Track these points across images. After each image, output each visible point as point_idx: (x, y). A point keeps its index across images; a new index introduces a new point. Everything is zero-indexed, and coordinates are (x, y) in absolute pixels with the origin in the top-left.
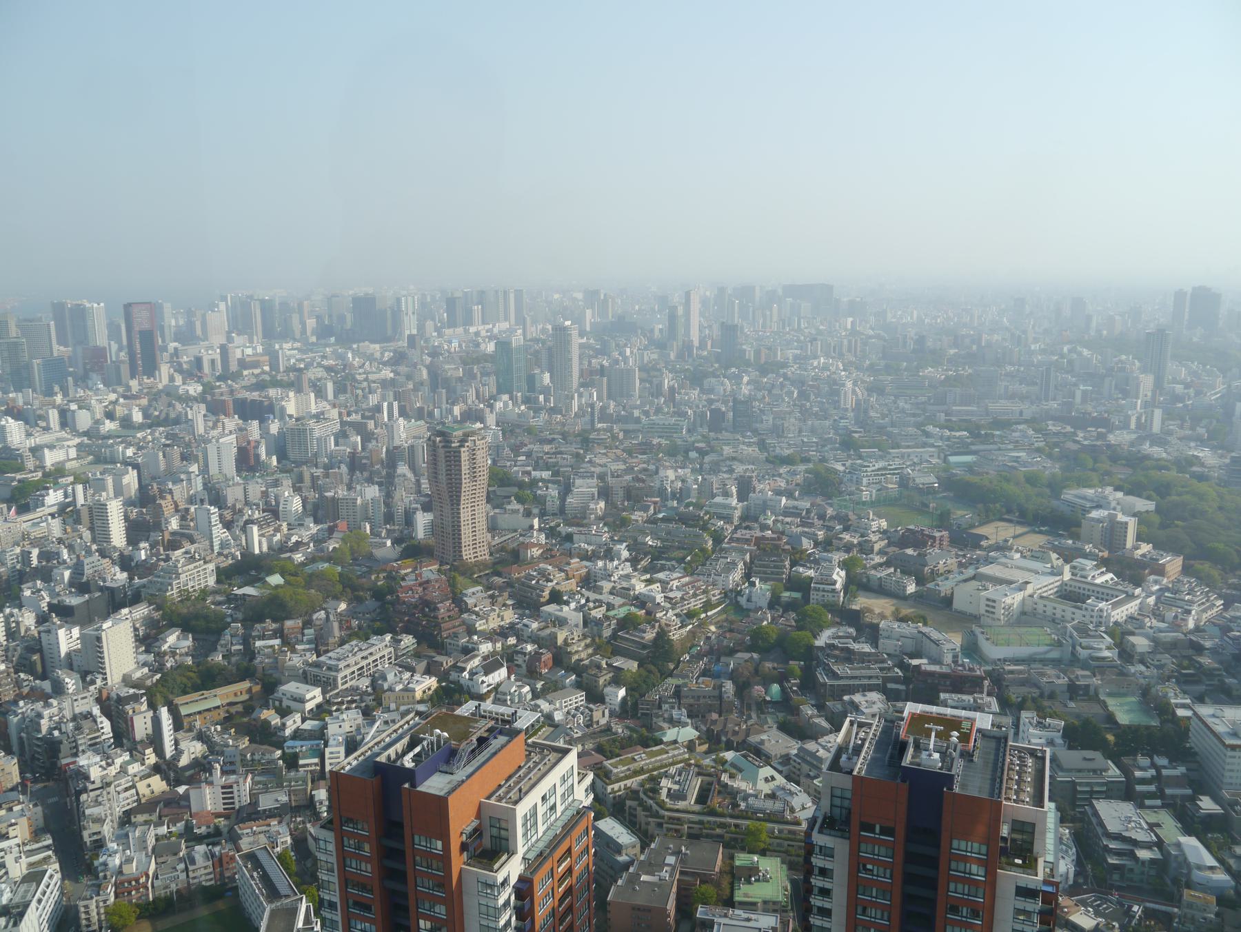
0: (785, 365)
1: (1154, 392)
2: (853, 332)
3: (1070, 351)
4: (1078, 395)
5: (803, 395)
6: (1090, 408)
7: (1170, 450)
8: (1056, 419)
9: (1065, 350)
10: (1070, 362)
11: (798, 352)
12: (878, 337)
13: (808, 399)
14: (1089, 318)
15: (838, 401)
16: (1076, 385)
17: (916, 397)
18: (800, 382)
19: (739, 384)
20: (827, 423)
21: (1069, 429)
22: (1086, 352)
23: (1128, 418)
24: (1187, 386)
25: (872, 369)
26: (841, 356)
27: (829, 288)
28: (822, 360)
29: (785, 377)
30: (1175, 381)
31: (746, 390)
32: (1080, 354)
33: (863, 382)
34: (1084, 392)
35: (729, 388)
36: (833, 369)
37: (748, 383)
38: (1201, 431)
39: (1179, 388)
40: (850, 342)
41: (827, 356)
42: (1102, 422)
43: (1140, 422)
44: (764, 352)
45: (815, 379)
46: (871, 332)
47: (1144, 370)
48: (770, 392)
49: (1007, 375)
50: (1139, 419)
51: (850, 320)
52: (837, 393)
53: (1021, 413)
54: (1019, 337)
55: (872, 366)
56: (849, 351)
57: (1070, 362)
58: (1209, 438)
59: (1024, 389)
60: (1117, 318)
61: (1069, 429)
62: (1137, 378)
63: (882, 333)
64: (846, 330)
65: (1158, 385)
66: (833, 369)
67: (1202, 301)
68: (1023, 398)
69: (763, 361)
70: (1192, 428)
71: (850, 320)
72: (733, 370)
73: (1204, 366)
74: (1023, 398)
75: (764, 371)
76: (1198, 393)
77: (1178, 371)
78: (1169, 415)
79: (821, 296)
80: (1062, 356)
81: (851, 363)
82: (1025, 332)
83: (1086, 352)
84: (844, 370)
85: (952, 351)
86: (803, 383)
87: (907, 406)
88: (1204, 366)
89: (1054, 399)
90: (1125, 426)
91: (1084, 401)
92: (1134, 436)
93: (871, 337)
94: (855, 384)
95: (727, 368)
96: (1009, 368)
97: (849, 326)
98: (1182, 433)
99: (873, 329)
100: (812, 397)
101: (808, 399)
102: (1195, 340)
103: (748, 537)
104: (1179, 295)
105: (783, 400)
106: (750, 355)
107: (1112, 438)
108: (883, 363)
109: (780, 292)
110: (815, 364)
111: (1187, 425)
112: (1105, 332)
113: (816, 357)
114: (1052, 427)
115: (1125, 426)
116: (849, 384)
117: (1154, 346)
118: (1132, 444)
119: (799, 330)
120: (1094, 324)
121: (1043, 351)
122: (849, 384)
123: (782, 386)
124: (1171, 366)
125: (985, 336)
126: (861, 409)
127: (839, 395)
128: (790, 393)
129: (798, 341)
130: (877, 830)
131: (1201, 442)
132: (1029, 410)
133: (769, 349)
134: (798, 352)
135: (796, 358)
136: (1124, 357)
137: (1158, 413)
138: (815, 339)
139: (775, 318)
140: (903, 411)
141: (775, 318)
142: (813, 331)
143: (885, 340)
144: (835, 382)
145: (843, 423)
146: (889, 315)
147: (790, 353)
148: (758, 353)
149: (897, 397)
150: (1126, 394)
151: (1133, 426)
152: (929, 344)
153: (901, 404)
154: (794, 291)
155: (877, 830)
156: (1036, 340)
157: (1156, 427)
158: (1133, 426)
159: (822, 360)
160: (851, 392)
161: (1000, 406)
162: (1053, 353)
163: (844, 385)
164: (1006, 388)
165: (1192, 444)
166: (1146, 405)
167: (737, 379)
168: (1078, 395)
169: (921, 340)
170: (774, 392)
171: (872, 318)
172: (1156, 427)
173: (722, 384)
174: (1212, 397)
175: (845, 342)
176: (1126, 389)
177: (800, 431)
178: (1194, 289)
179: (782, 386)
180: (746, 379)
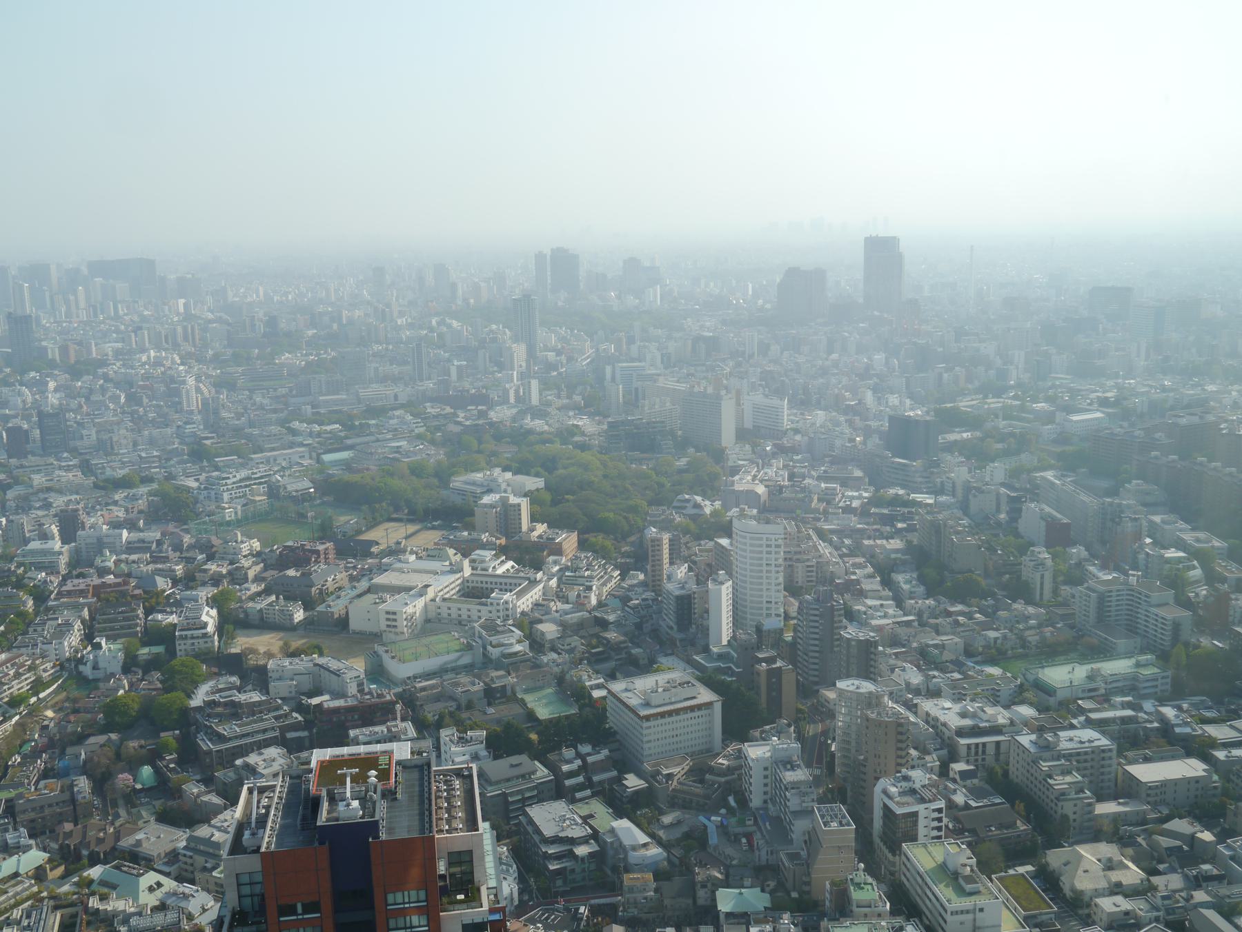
0: (103, 363)
1: (528, 361)
2: (188, 316)
3: (439, 324)
5: (133, 399)
6: (467, 385)
8: (432, 400)
9: (434, 322)
10: (440, 336)
11: (120, 345)
12: (219, 320)
13: (140, 404)
14: (454, 286)
15: (180, 403)
16: (449, 360)
17: (275, 390)
18: (127, 384)
19: (43, 392)
20: (169, 431)
21: (448, 410)
22: (455, 324)
23: (506, 392)
24: (559, 353)
25: (217, 360)
26: (176, 346)
27: (149, 264)
28: (152, 353)
29: (106, 378)
30: (546, 349)
31: (53, 399)
32: (449, 326)
33: (208, 376)
35: (30, 399)
36: (168, 363)
37: (56, 390)
39: (551, 356)
40: (185, 328)
41: (158, 348)
42: (481, 399)
43: (518, 394)
44: (73, 349)
45: (146, 377)
46: (210, 316)
47: (516, 339)
48: (87, 399)
49: (374, 355)
50: (517, 392)
51: (182, 301)
52: (177, 392)
53: (396, 397)
54: (383, 311)
55: (216, 356)
56: (186, 339)
57: (440, 336)
58: (586, 406)
59: (395, 369)
60: (483, 284)
61: (448, 410)
62: (510, 348)
63: (225, 317)
64: (178, 314)
66: (168, 363)
67: (561, 264)
68: (396, 380)
69: (72, 360)
70: (569, 397)
71: (182, 301)
72: (32, 374)
73: (572, 330)
74: (396, 380)
75: (75, 373)
76: (570, 359)
77: (547, 337)
78: (545, 385)
79: (141, 274)
80: (431, 330)
81: (190, 355)
82: (388, 305)
83: (455, 324)
84: (182, 364)
85: (310, 333)
86: (131, 385)
87: (266, 401)
88: (572, 330)
89: (429, 379)
90: (505, 401)
91: (460, 378)
92: (514, 411)
93: (210, 321)
94: (198, 379)
95: (24, 372)
96: (376, 347)
97: (181, 309)
98: (560, 403)
99: (212, 312)
100: (145, 400)
101: (140, 404)
102: (560, 304)
103: (82, 587)
104: (540, 257)
105: (107, 408)
106: (54, 353)
108: (229, 351)
109: (85, 270)
110: (144, 358)
111: (564, 394)
112: (472, 301)
113: (143, 350)
114: (431, 410)
115: (505, 401)
116: (191, 381)
117: (522, 313)
118: (514, 419)
119: (117, 317)
120: (460, 292)
121: (410, 326)
122: (191, 381)
123: (103, 390)
124: (541, 333)
125: (345, 313)
126: (210, 410)
127: (180, 396)
128: (115, 399)
129: (117, 331)
130: (300, 910)
131: (580, 410)
132: (404, 393)
133: (80, 344)
134: (120, 345)
135: (118, 353)
136: (494, 327)
137: (535, 384)
138: (140, 328)
139: (82, 304)
140: (262, 407)
141: (82, 304)
142: (136, 318)
143: (229, 324)
144: (172, 380)
145: (189, 429)
146: (230, 294)
147: (109, 348)
148: (64, 350)
149: (251, 391)
150: (501, 366)
151: (512, 400)
152: (283, 325)
153: (258, 399)
154: (102, 268)
155: (300, 910)
156: (401, 314)
157: (535, 400)
158: (512, 400)
159: (152, 353)
160: (195, 391)
161: (372, 392)
163: (184, 382)
164: (376, 369)
165: (571, 413)
166: (522, 376)
167: (40, 386)
169: (272, 322)
170: (94, 398)
171: (209, 299)
172: (535, 400)
173: (20, 394)
174: (583, 362)
175: (179, 329)
176: (501, 361)
177: (135, 444)
178: (552, 250)
179: (103, 390)
180: (52, 385)
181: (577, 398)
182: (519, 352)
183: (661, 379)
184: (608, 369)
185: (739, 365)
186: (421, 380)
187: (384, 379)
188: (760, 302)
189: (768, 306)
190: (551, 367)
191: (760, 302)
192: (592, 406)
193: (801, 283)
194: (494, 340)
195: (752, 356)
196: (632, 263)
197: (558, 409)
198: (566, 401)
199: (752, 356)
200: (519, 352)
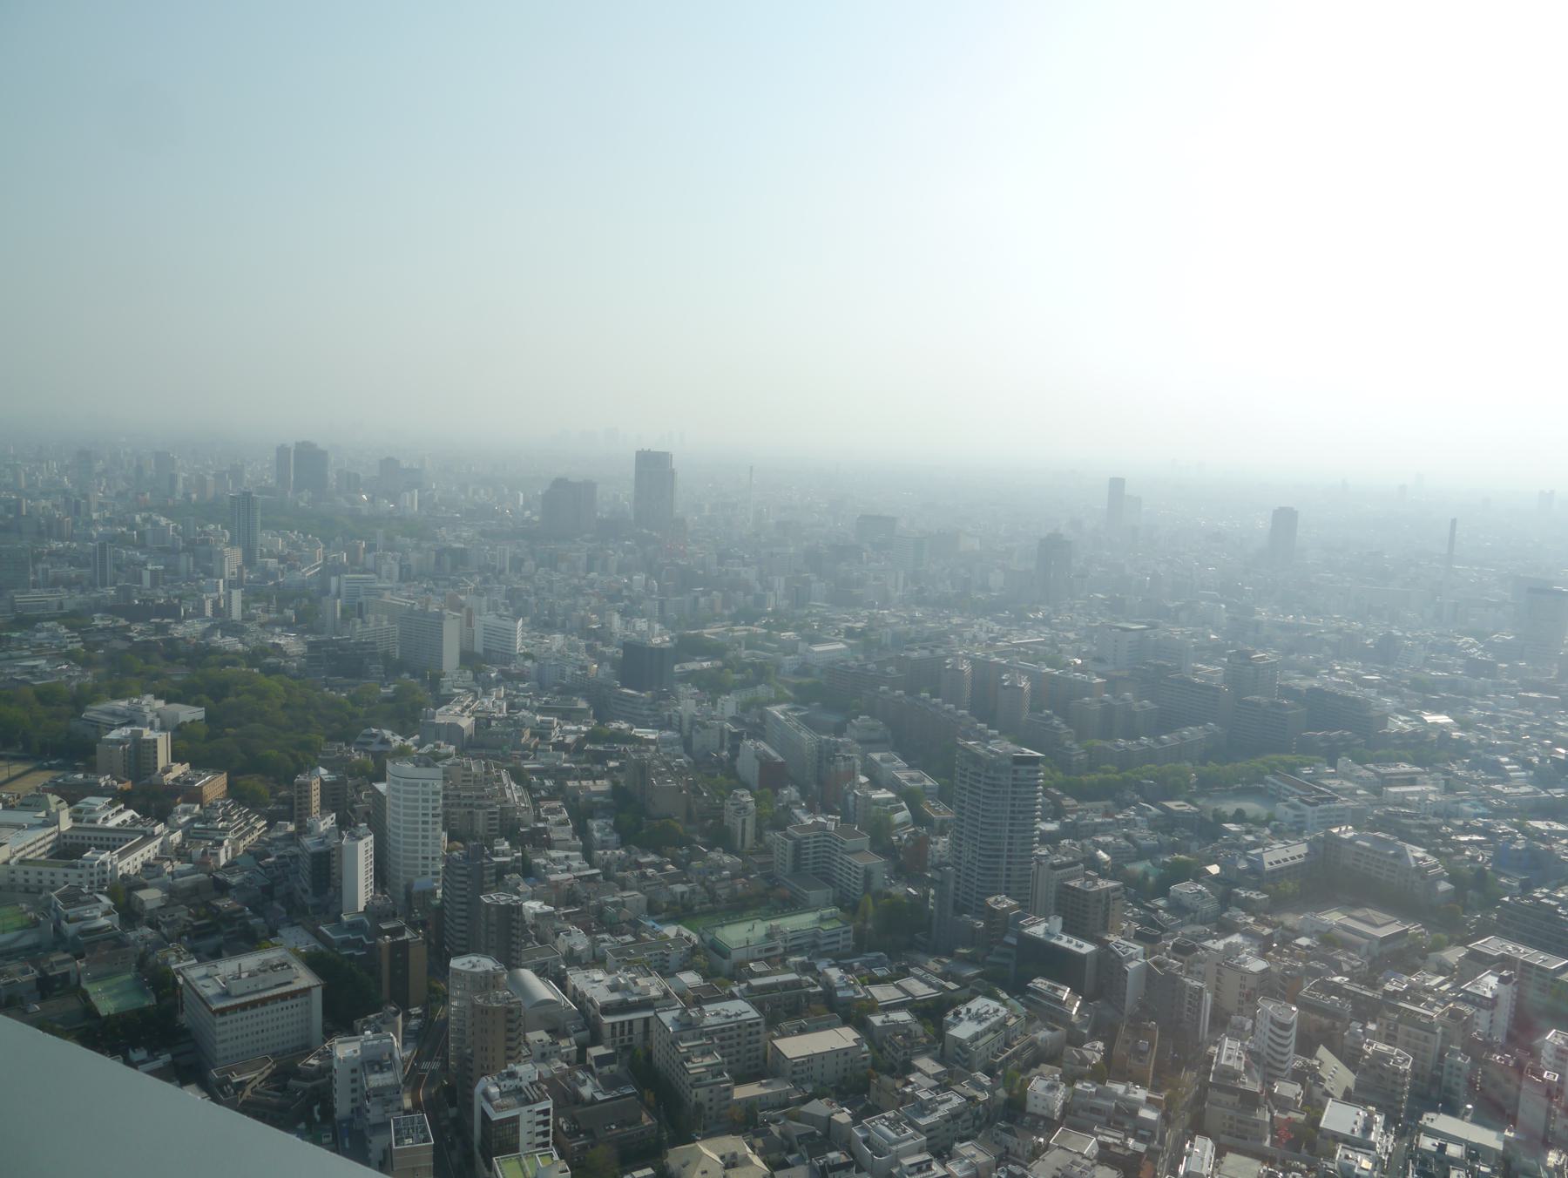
1: (239, 568)
3: (145, 520)
4: (146, 577)
6: (160, 592)
7: (248, 639)
8: (111, 610)
9: (138, 518)
10: (141, 535)
14: (173, 479)
16: (145, 564)
21: (122, 622)
22: (163, 521)
23: (202, 603)
30: (271, 555)
32: (156, 523)
34: (154, 573)
38: (290, 613)
39: (272, 563)
42: (171, 611)
43: (217, 607)
47: (231, 543)
49: (51, 554)
50: (216, 604)
53: (61, 606)
54: (77, 503)
57: (141, 535)
58: (299, 621)
59: (73, 572)
61: (122, 622)
62: (222, 552)
65: (249, 561)
67: (305, 460)
68: (69, 584)
70: (280, 611)
73: (305, 535)
74: (69, 584)
77: (272, 541)
78: (253, 594)
80: (132, 527)
82: (85, 496)
83: (163, 521)
88: (305, 535)
89: (114, 584)
90: (199, 613)
91: (154, 584)
92: (208, 625)
96: (56, 545)
98: (265, 618)
102: (302, 504)
104: (282, 451)
107: (178, 631)
111: (273, 607)
112: (194, 496)
114: (99, 621)
115: (199, 613)
117: (242, 512)
118: (205, 635)
120: (180, 485)
121: (109, 522)
131: (288, 626)
132: (72, 599)
136: (212, 527)
137: (237, 595)
150: (209, 573)
151: (209, 613)
157: (236, 613)
158: (209, 613)
161: (29, 598)
162: (121, 524)
164: (45, 571)
165: (278, 630)
166: (231, 585)
168: (146, 577)
172: (236, 613)
174: (308, 572)
176: (207, 564)
181: (290, 613)
182: (233, 558)
183: (387, 593)
184: (334, 581)
185: (486, 580)
186: (104, 585)
187: (55, 583)
188: (528, 513)
189: (536, 518)
190: (267, 574)
191: (528, 513)
192: (304, 622)
193: (567, 498)
194: (205, 542)
195: (502, 571)
196: (389, 465)
197: (262, 625)
198: (274, 616)
199: (502, 571)
200: (233, 558)
